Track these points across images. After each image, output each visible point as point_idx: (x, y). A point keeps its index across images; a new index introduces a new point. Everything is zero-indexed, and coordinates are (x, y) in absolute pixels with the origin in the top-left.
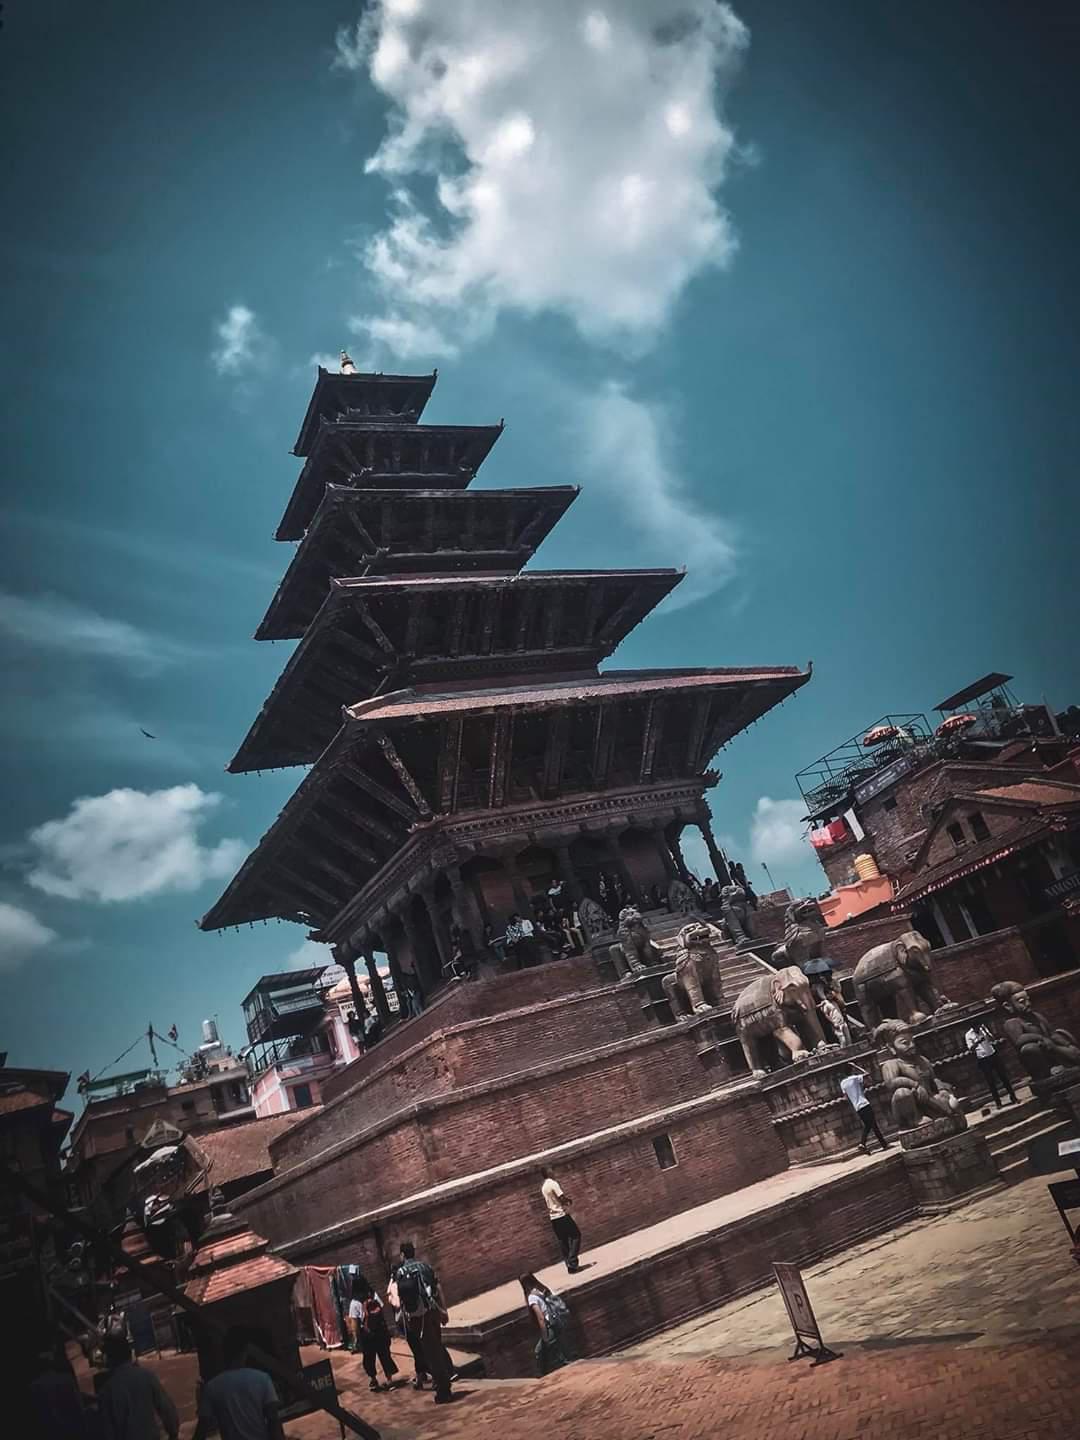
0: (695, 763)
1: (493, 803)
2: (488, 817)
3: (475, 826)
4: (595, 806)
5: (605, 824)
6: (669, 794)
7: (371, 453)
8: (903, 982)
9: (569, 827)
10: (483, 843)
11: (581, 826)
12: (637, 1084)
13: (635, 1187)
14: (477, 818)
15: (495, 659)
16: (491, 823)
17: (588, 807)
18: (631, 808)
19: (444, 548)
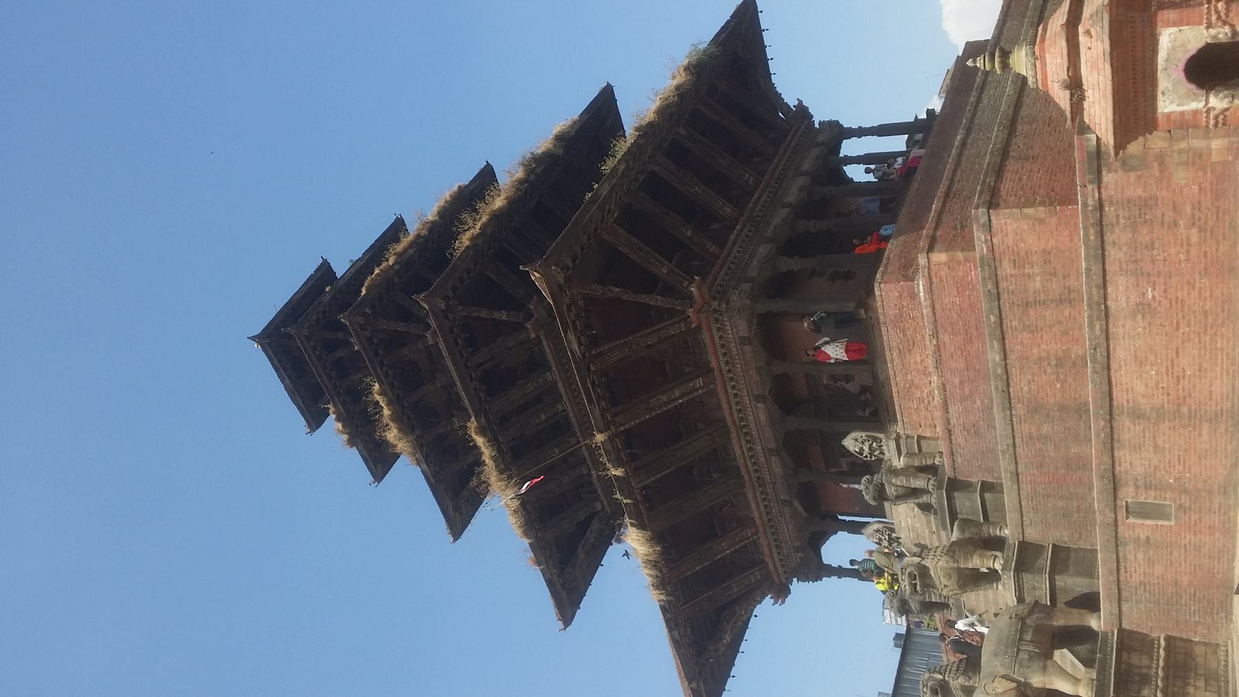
0: (678, 322)
2: (769, 545)
4: (748, 442)
6: (725, 354)
16: (775, 540)
17: (750, 449)
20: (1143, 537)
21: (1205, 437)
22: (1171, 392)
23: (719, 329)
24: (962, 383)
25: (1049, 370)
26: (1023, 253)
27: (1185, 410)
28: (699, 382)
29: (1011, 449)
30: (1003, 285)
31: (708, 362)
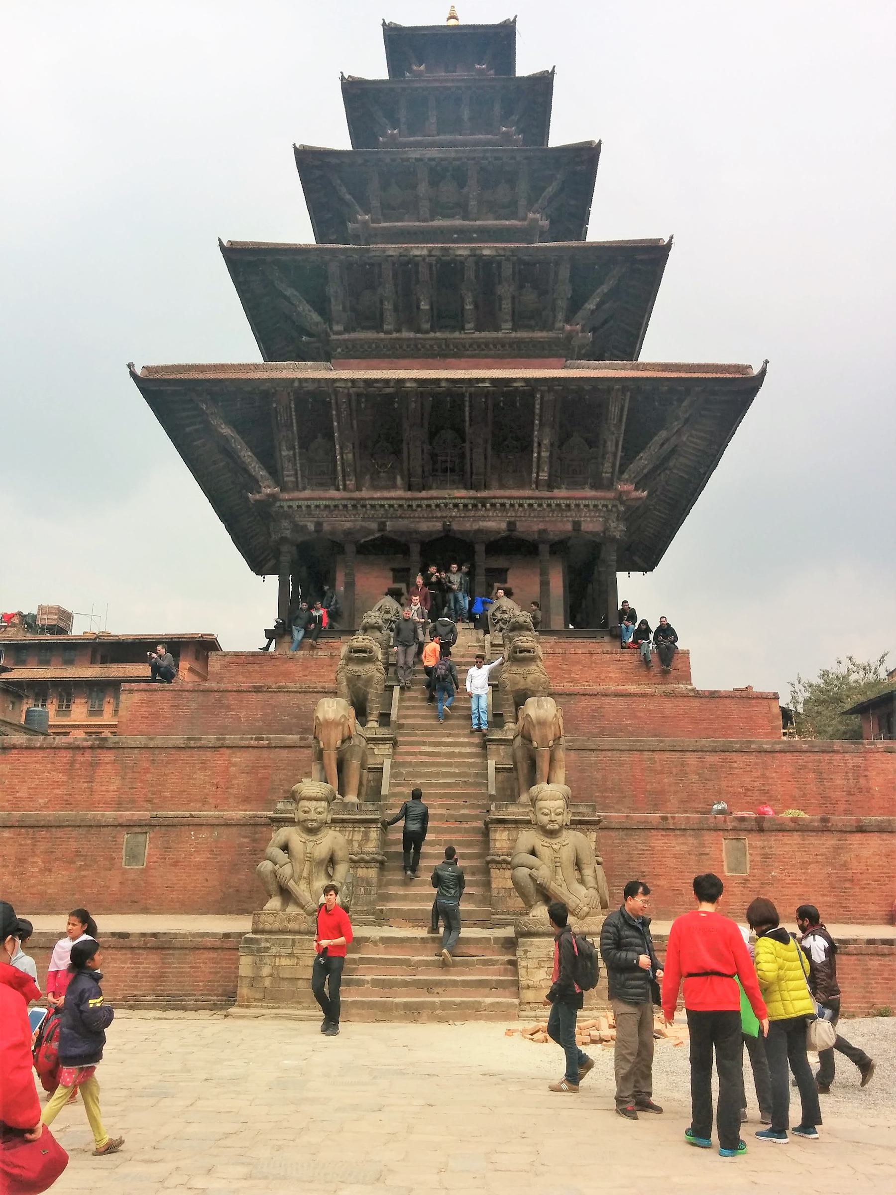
0: (612, 473)
1: (345, 485)
3: (317, 506)
4: (465, 506)
5: (475, 527)
6: (568, 506)
7: (403, 115)
8: (519, 754)
9: (430, 524)
10: (325, 525)
11: (444, 525)
12: (235, 782)
13: (83, 873)
14: (321, 499)
15: (432, 339)
16: (336, 506)
17: (456, 506)
18: (514, 514)
19: (444, 216)
20: (707, 850)
21: (821, 899)
22: (864, 876)
23: (595, 506)
24: (649, 710)
25: (756, 784)
26: (867, 773)
27: (848, 885)
28: (544, 476)
29: (670, 748)
30: (838, 757)
31: (559, 488)
